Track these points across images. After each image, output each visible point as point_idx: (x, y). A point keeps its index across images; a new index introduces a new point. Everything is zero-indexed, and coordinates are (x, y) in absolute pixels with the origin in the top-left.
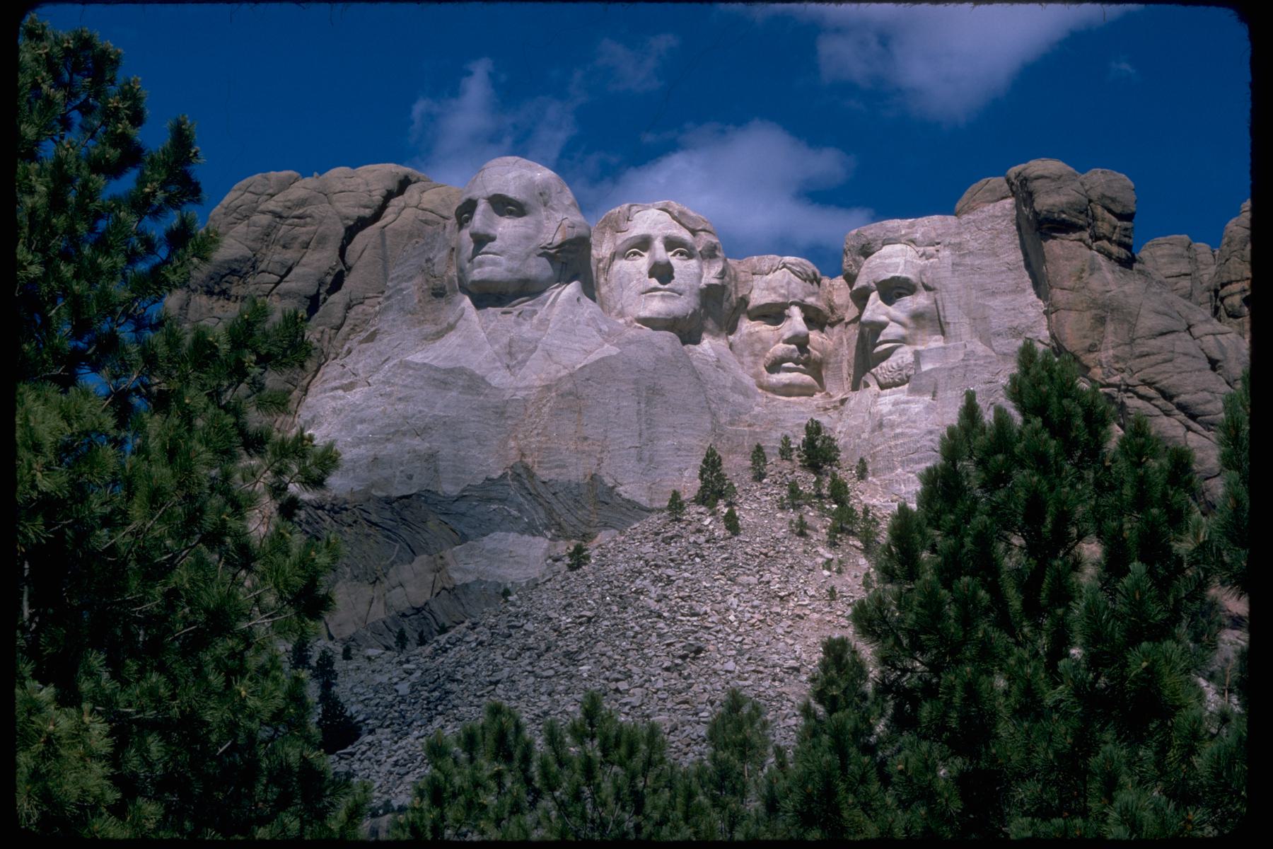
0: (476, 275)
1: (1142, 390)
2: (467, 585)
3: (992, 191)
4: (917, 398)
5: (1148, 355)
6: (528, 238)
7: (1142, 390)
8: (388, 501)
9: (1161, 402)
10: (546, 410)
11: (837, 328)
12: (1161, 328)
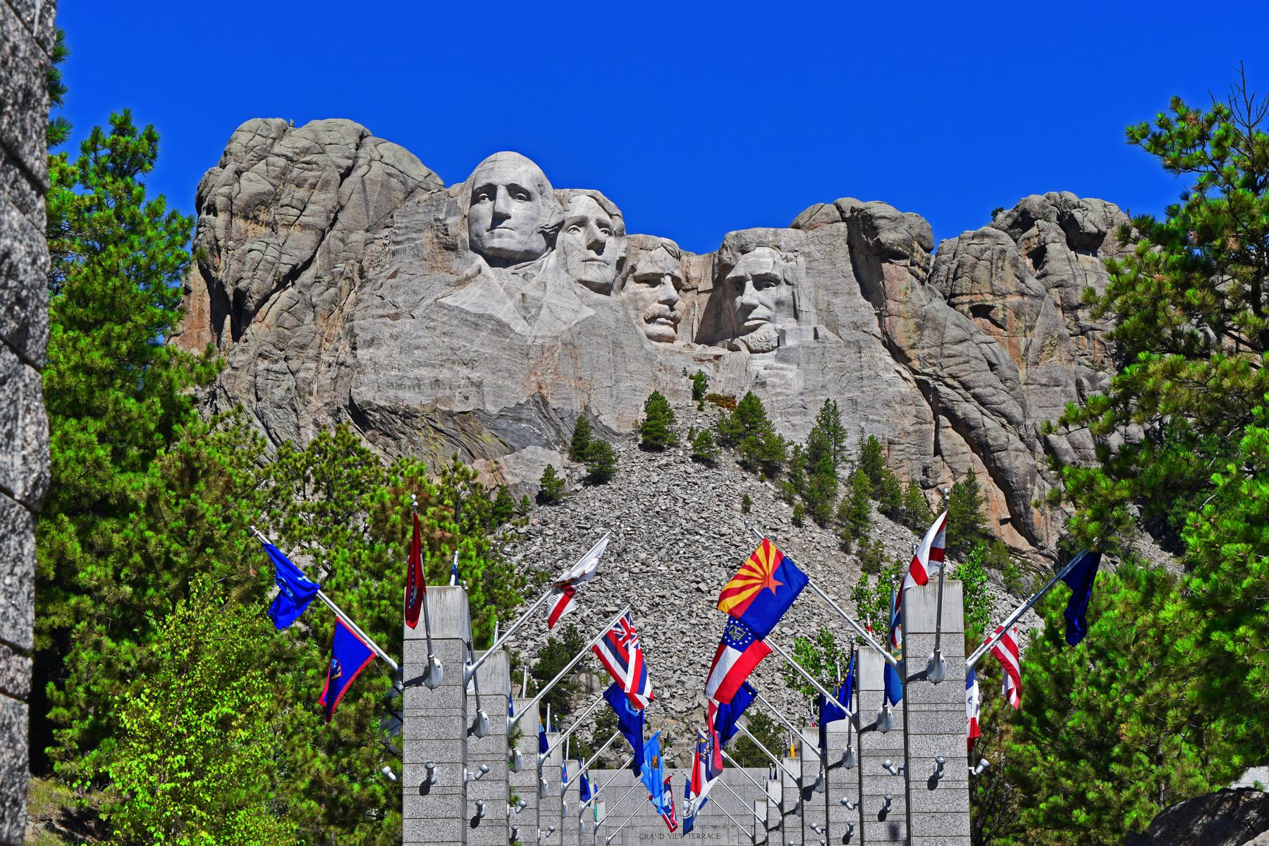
0: (496, 243)
1: (950, 381)
2: (516, 485)
3: (827, 214)
4: (785, 366)
5: (954, 356)
6: (533, 219)
7: (950, 381)
8: (450, 414)
9: (962, 391)
10: (556, 355)
11: (689, 294)
12: (960, 337)
